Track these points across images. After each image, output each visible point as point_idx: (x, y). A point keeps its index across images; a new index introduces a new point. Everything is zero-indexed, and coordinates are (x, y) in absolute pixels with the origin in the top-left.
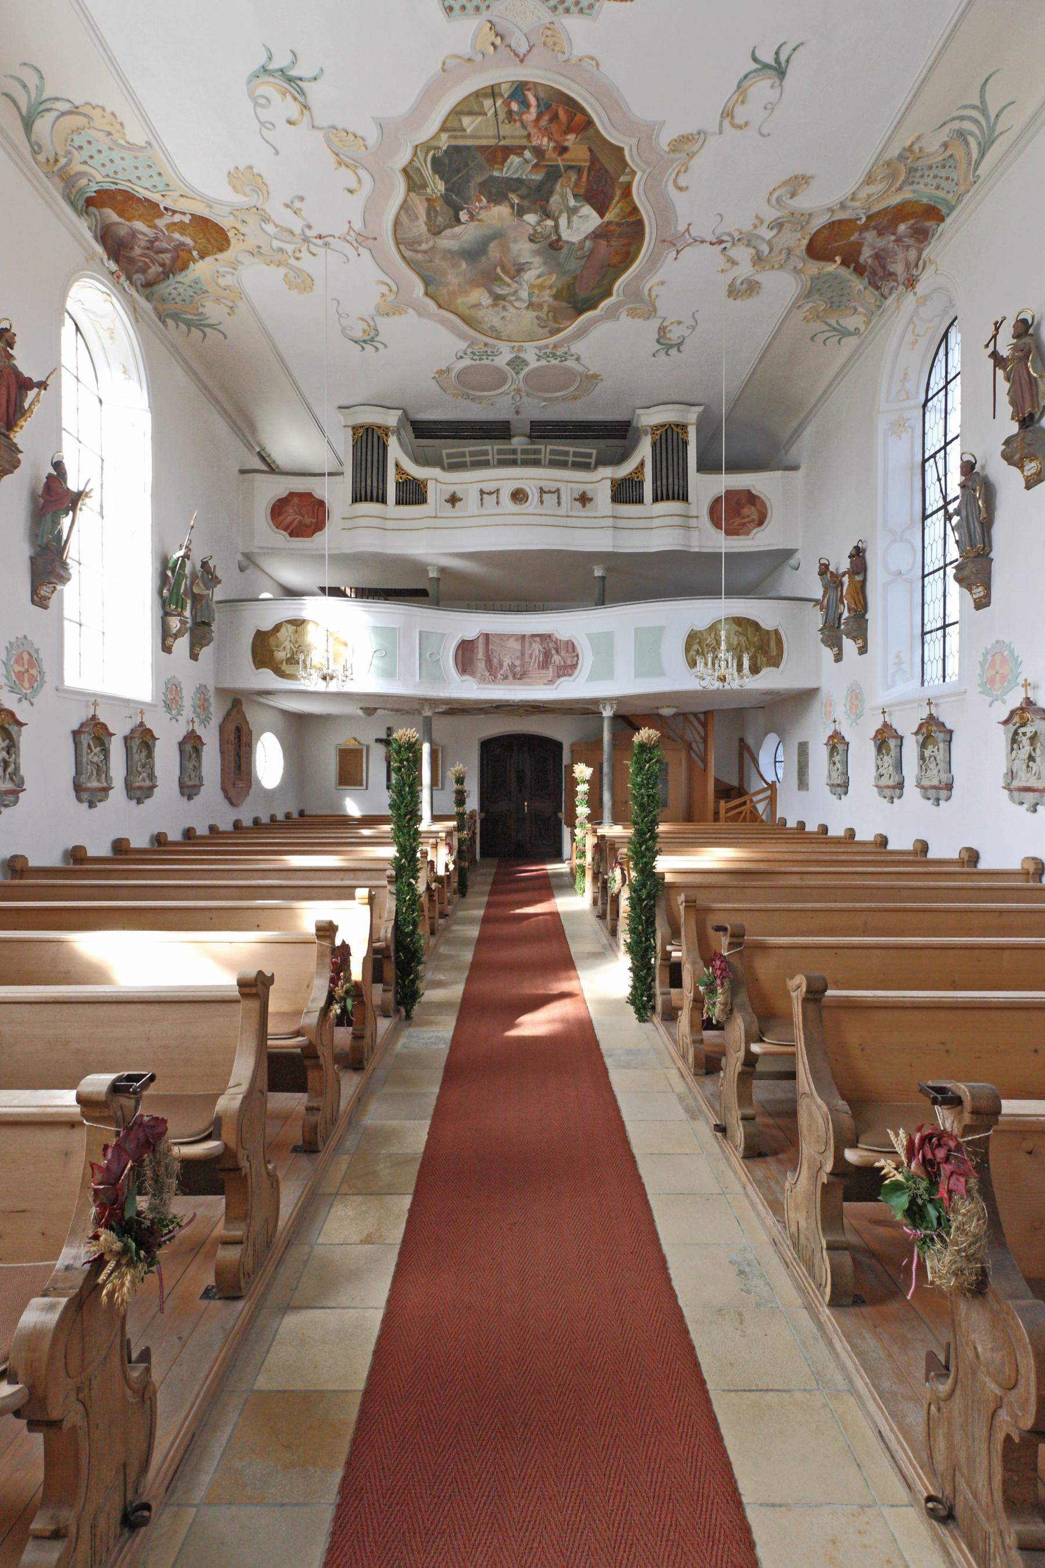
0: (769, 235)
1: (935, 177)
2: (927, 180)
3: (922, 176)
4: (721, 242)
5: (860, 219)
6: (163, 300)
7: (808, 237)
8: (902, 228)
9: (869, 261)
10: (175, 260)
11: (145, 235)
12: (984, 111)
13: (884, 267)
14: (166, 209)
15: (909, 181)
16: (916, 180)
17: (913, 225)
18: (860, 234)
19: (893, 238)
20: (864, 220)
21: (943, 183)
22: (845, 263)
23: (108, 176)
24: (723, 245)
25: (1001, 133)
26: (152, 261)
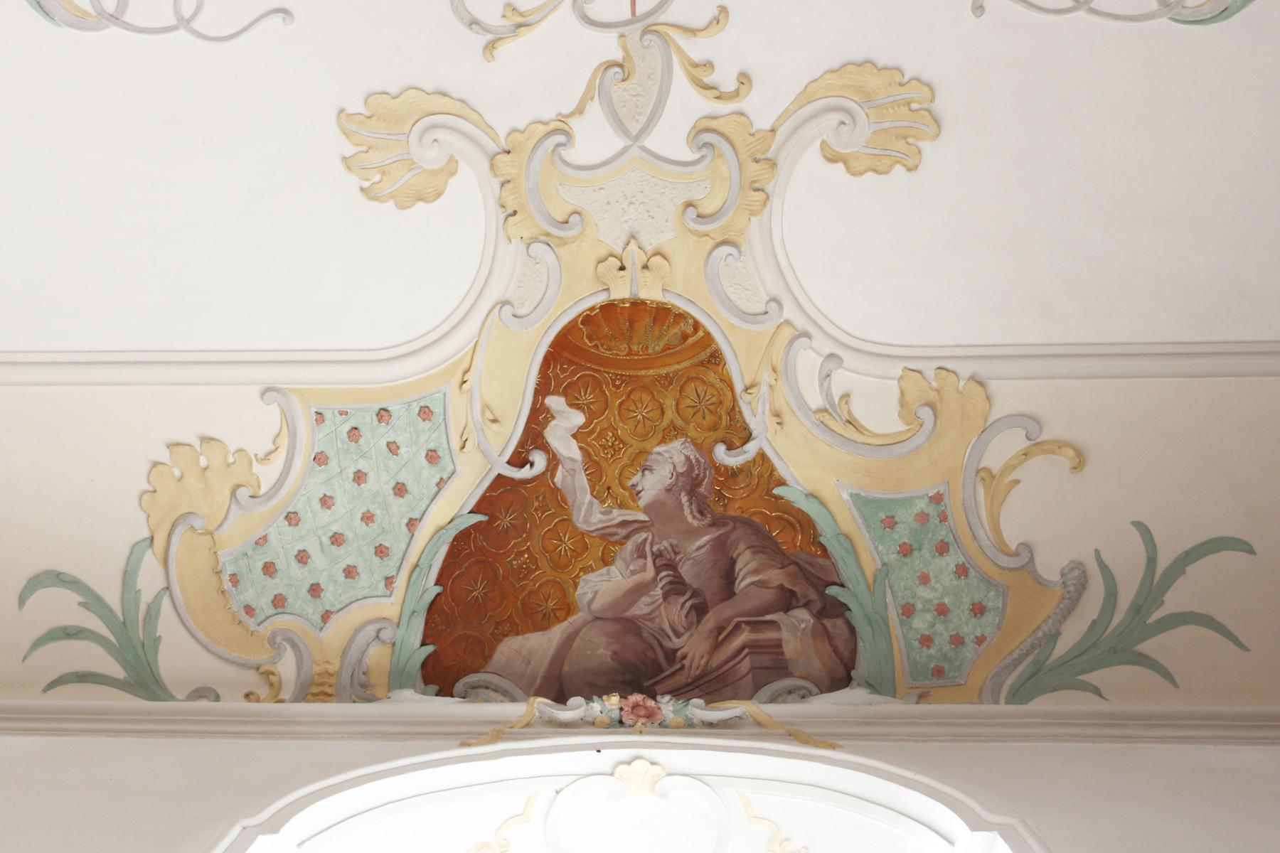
6: (939, 672)
10: (766, 546)
11: (641, 590)
14: (519, 460)
23: (389, 581)
26: (755, 626)
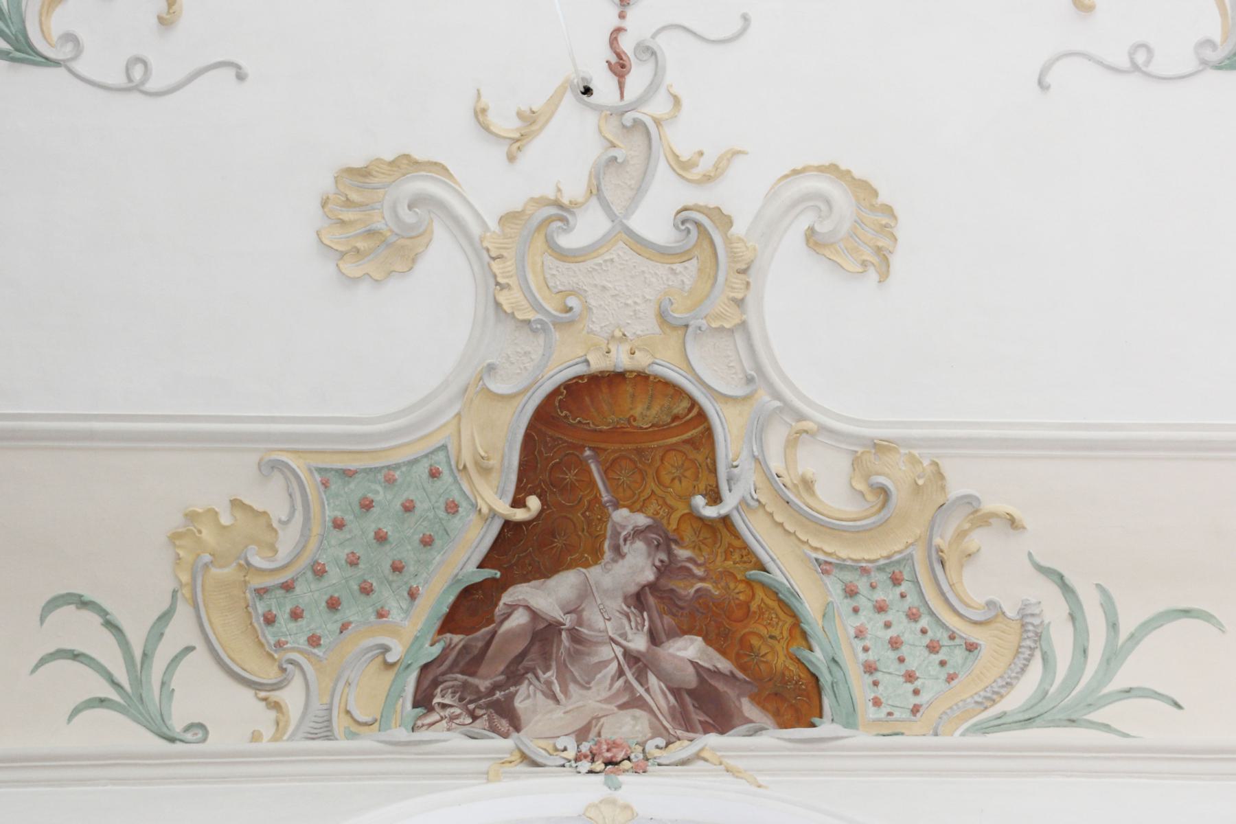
0: (654, 221)
1: (895, 644)
2: (873, 623)
3: (881, 608)
4: (620, 68)
5: (715, 497)
7: (642, 361)
8: (688, 650)
9: (519, 619)
12: (1113, 658)
13: (514, 675)
15: (851, 578)
16: (861, 601)
17: (717, 673)
18: (638, 533)
19: (639, 643)
20: (711, 512)
21: (891, 682)
22: (510, 532)
24: (605, 85)
25: (1106, 727)
